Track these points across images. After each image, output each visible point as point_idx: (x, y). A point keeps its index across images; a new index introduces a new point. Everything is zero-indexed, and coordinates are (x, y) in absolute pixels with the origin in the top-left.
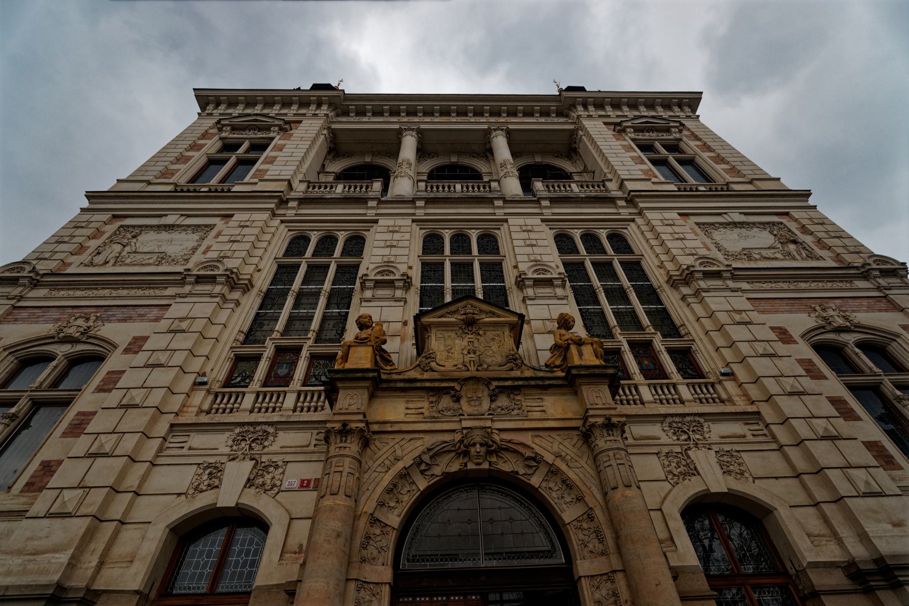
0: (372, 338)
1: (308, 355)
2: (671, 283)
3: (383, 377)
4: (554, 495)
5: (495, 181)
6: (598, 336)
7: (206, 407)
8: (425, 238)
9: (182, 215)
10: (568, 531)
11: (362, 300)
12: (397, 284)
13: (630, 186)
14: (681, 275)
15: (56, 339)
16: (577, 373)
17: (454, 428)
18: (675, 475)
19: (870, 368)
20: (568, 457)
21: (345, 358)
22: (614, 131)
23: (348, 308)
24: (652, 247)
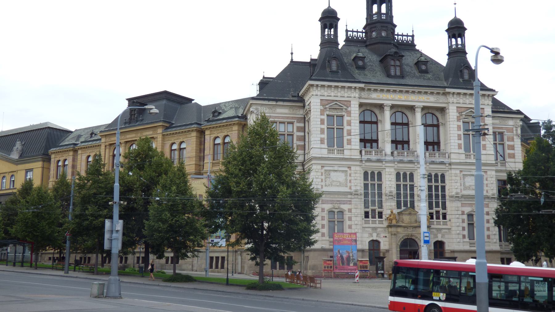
8: (397, 173)
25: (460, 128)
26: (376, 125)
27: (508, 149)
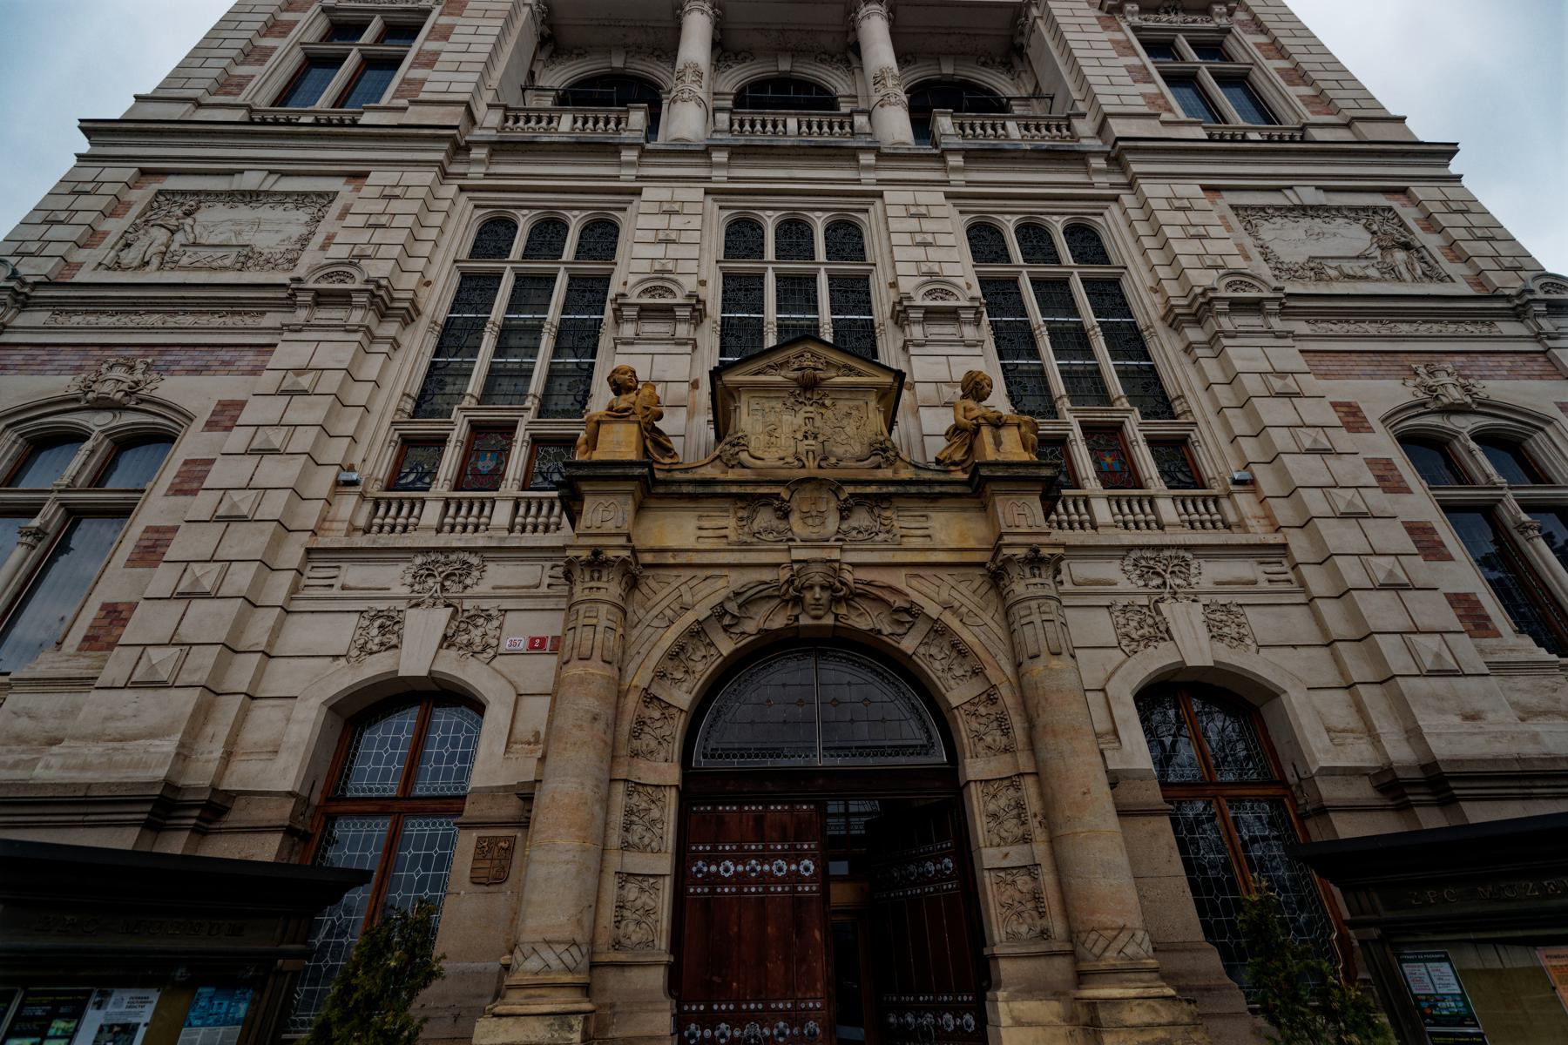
0: (638, 410)
1: (527, 437)
2: (1170, 320)
3: (659, 475)
4: (937, 665)
5: (862, 112)
6: (1031, 413)
7: (361, 521)
8: (729, 226)
9: (271, 172)
10: (955, 718)
11: (618, 341)
12: (679, 313)
13: (1119, 128)
14: (1189, 306)
15: (83, 403)
16: (988, 473)
17: (779, 561)
18: (1133, 640)
19: (1488, 477)
20: (964, 610)
21: (592, 443)
22: (1100, 8)
23: (594, 356)
24: (1144, 253)
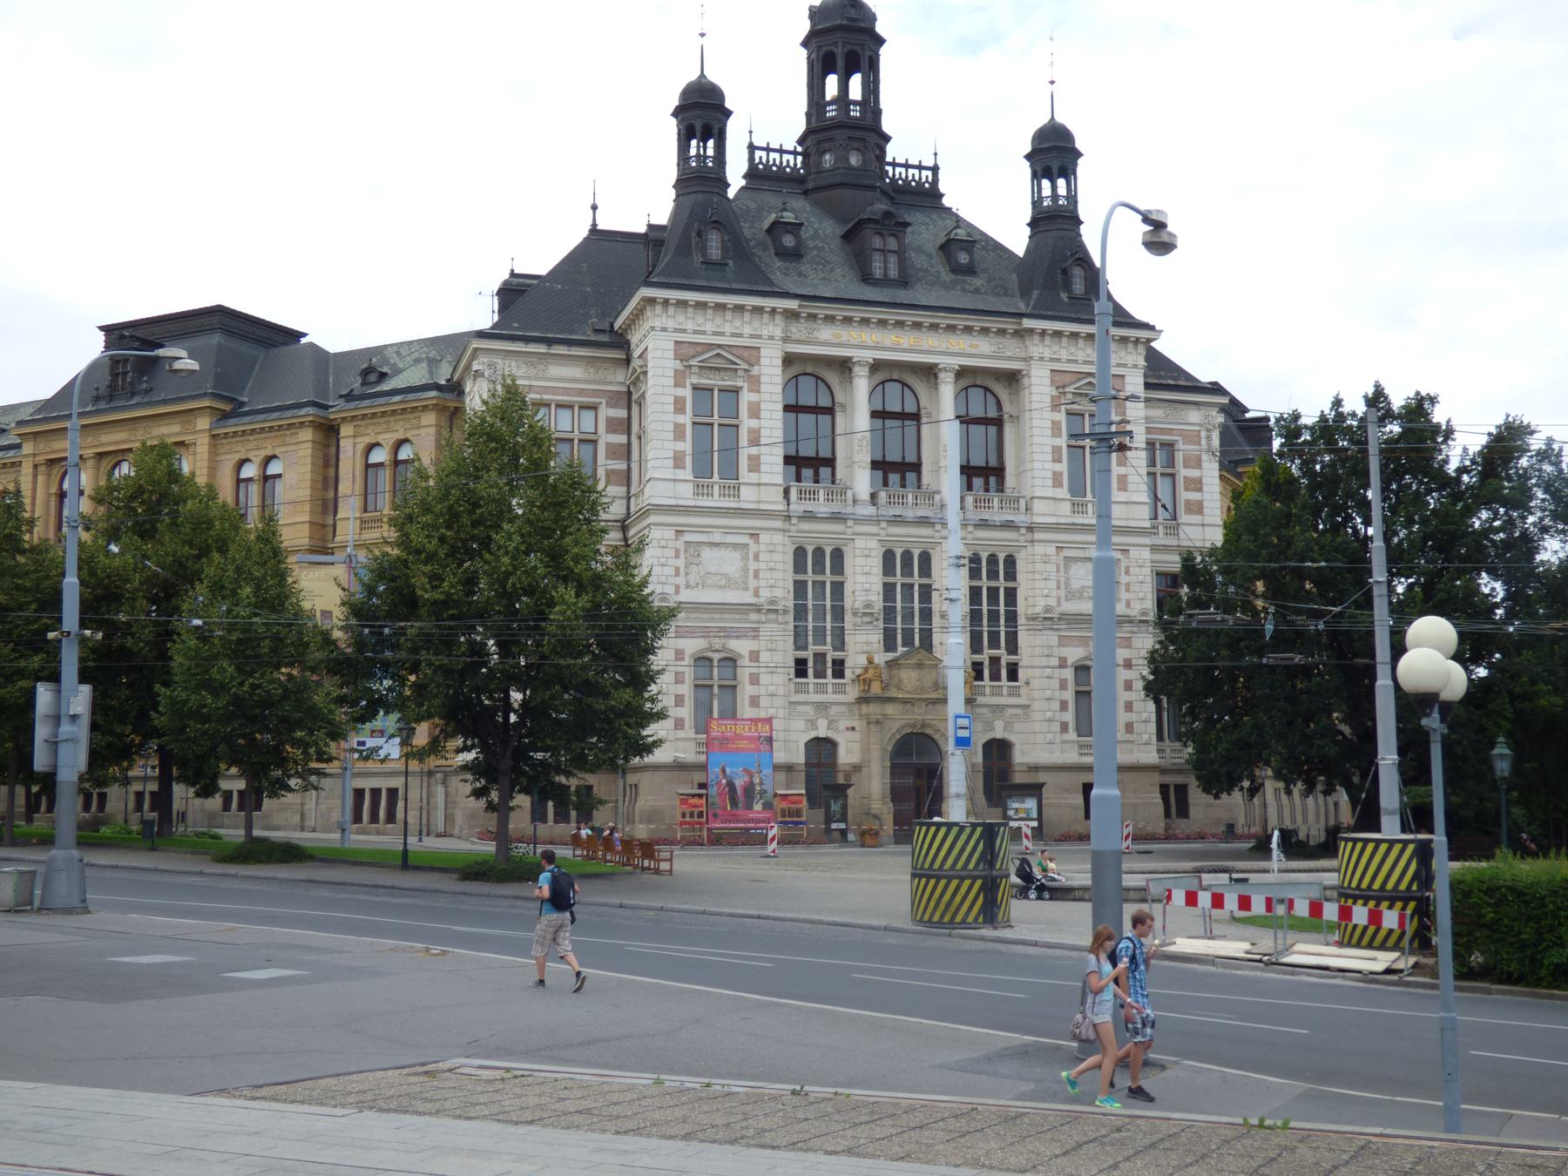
25: (1060, 429)
26: (829, 417)
27: (1186, 489)
